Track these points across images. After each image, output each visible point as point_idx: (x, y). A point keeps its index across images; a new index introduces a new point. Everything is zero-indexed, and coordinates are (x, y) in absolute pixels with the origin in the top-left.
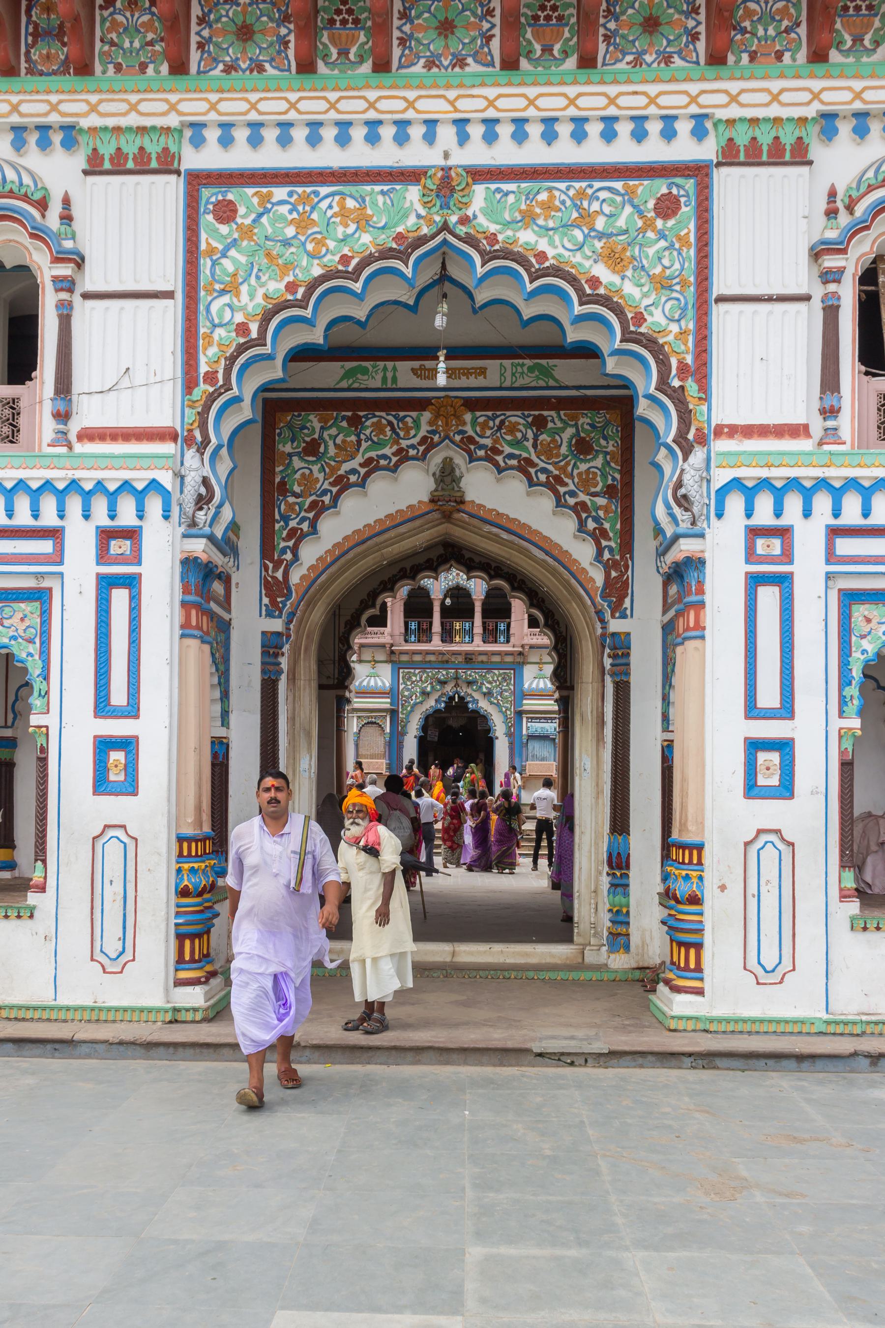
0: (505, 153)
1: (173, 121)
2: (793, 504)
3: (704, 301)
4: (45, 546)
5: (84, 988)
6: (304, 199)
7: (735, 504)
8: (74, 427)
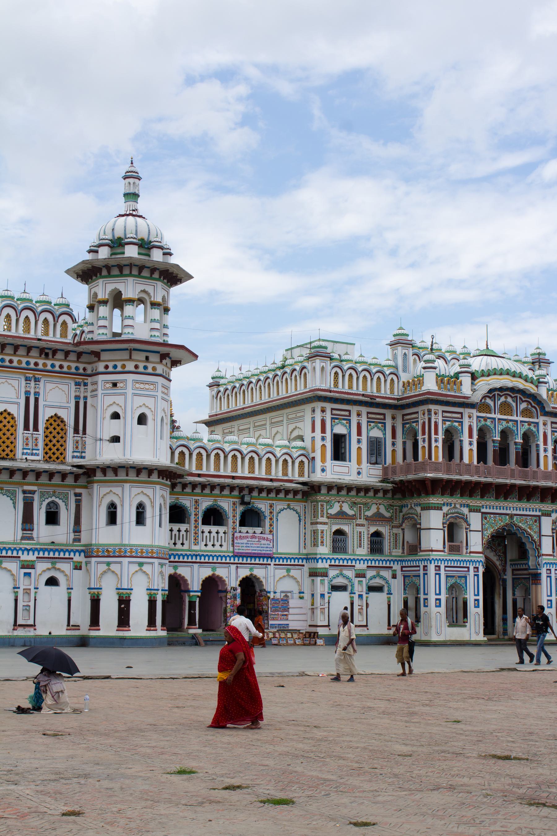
0: (518, 512)
1: (481, 505)
2: (551, 566)
3: (540, 536)
4: (466, 569)
6: (495, 517)
7: (545, 566)
8: (468, 551)
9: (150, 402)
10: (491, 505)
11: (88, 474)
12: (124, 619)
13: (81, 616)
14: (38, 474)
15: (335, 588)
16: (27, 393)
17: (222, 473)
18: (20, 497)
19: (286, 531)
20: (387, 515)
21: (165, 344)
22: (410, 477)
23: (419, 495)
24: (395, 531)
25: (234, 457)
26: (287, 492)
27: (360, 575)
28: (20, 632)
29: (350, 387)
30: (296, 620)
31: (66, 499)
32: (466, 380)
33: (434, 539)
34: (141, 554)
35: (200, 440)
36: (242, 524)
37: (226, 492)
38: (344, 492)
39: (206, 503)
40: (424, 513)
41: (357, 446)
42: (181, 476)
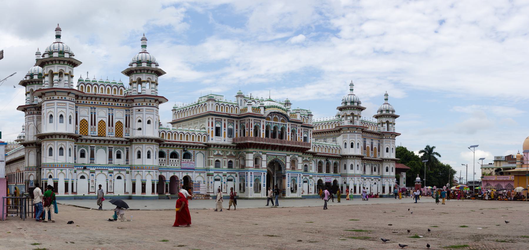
5: (263, 197)
9: (151, 116)
10: (270, 152)
11: (130, 141)
12: (144, 190)
13: (129, 189)
14: (114, 141)
15: (216, 180)
17: (177, 140)
18: (108, 149)
19: (199, 160)
20: (234, 155)
21: (157, 96)
22: (242, 142)
23: (245, 148)
24: (237, 160)
25: (181, 135)
26: (199, 147)
27: (225, 175)
28: (109, 195)
29: (222, 111)
30: (203, 190)
31: (123, 150)
32: (262, 109)
33: (250, 163)
34: (149, 168)
35: (169, 129)
36: (184, 158)
37: (178, 147)
38: (219, 147)
39: (171, 151)
40: (247, 155)
41: (224, 131)
42: (163, 142)
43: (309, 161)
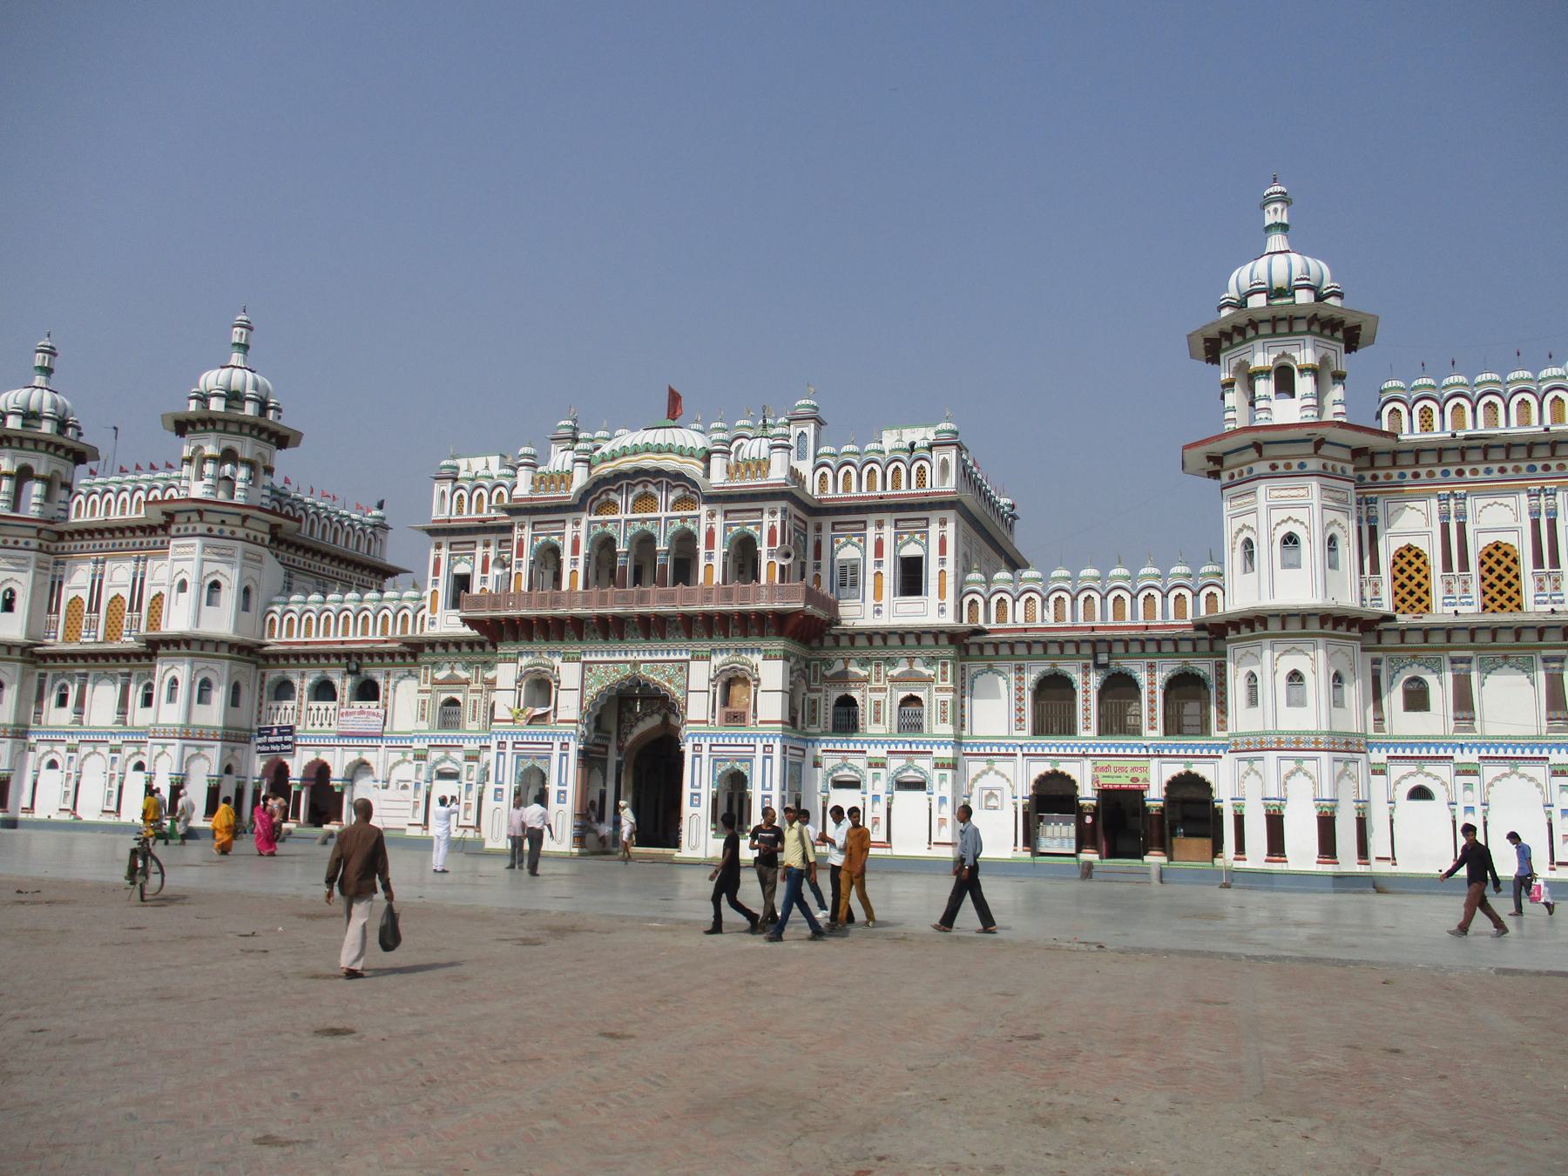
3: (688, 691)
9: (188, 566)
15: (443, 775)
16: (135, 574)
26: (403, 655)
43: (929, 680)
